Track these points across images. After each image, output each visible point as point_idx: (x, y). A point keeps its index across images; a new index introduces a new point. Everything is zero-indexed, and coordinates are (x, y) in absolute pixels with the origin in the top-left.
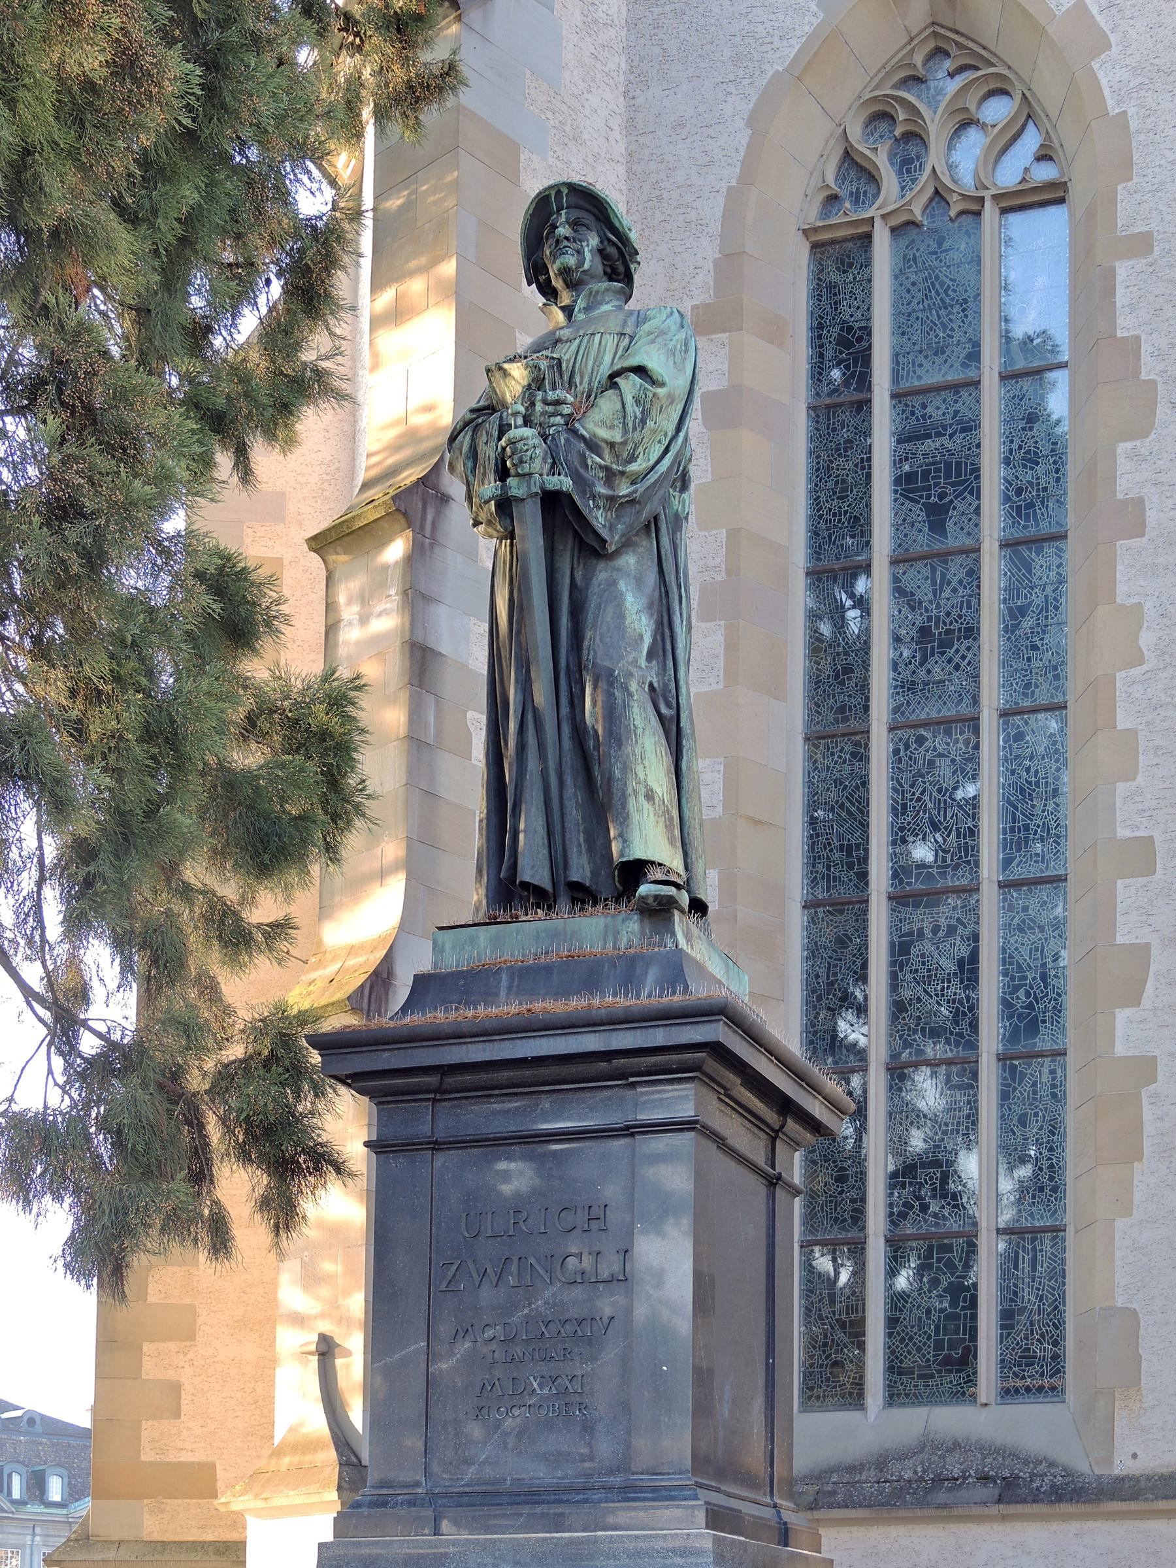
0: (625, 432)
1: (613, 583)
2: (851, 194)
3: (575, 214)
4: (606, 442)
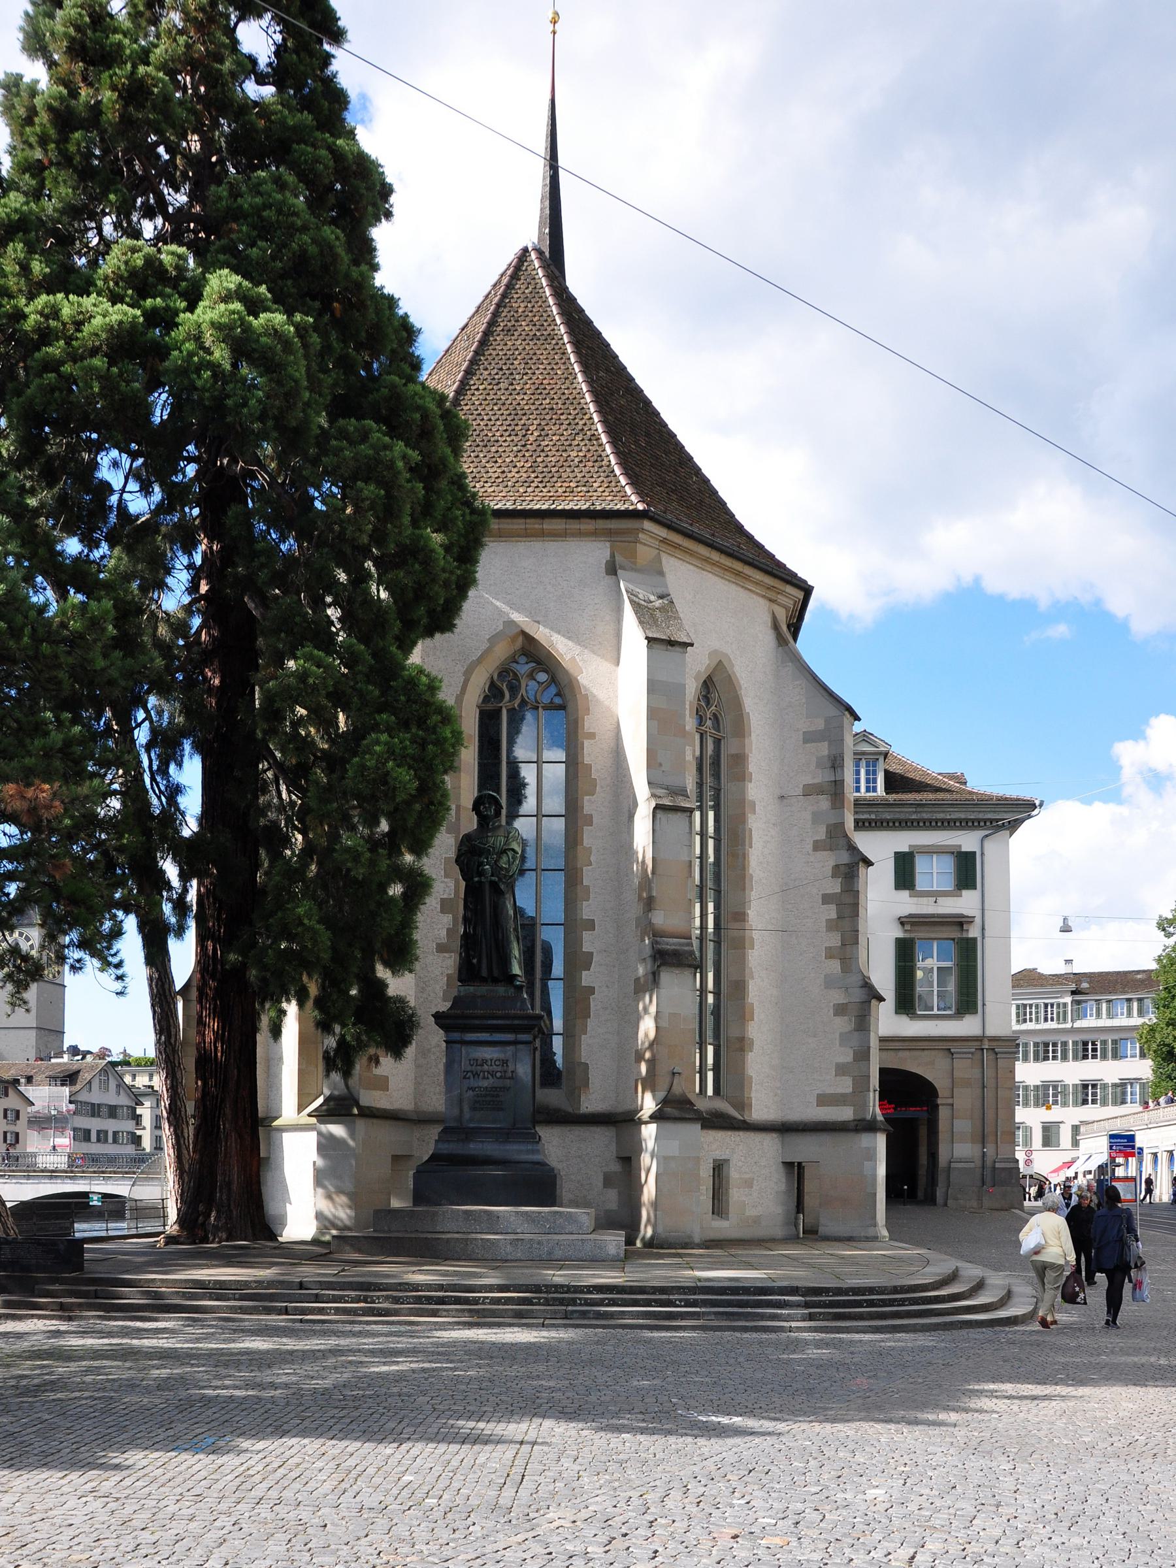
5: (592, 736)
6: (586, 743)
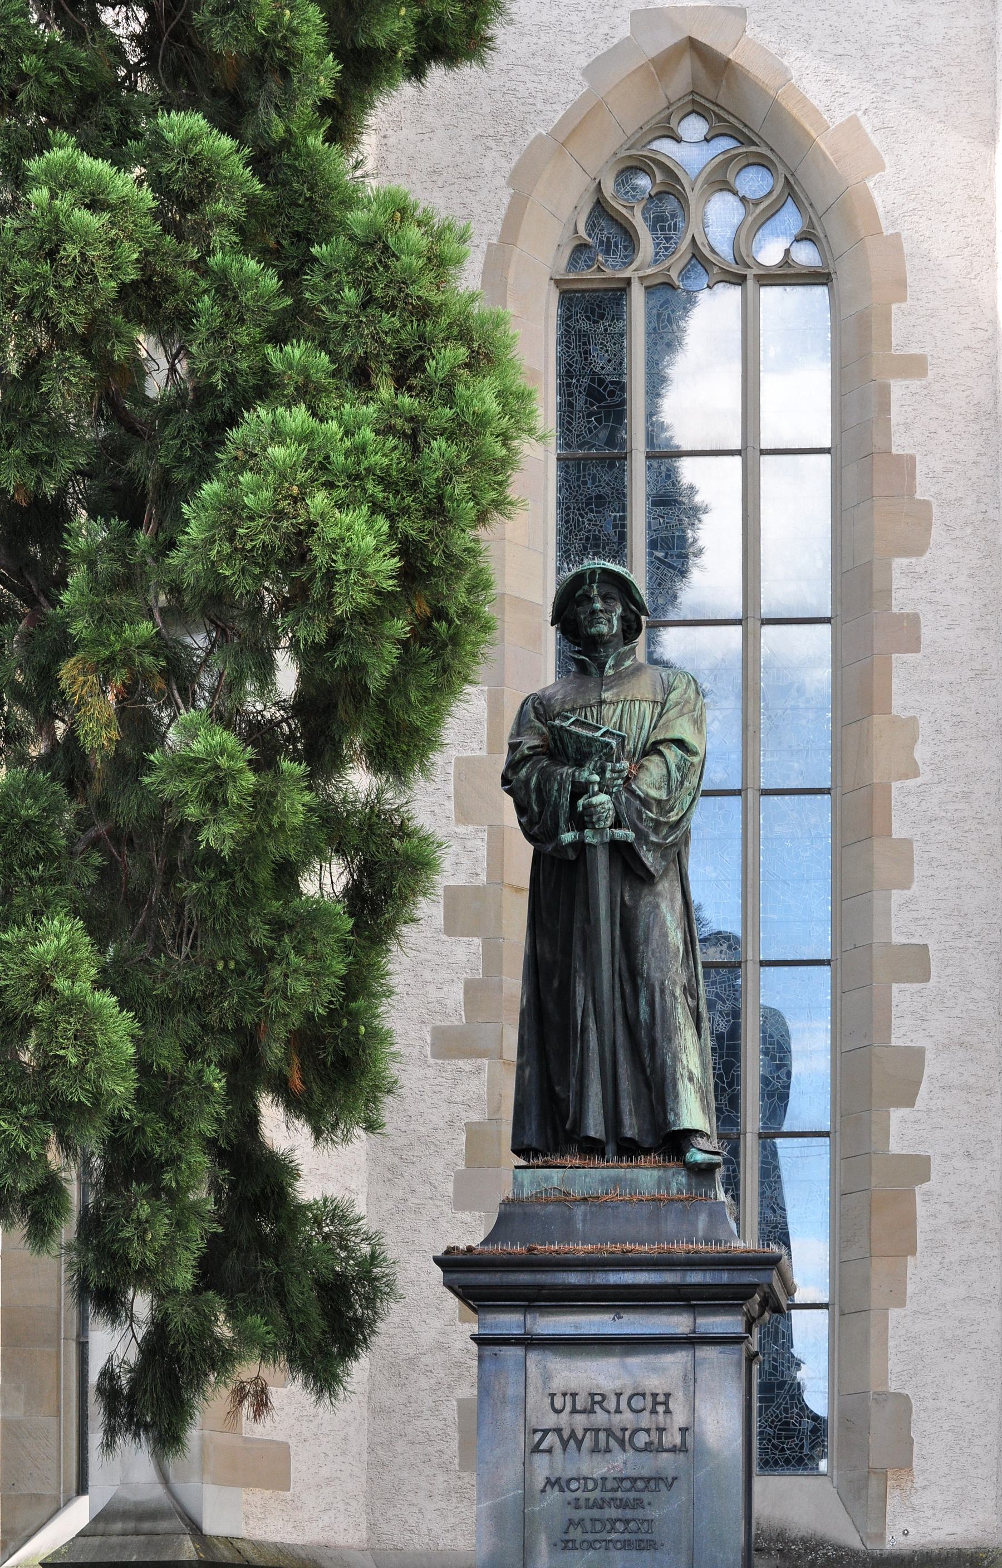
0: (669, 792)
1: (657, 906)
2: (601, 242)
3: (606, 589)
4: (655, 799)
5: (914, 366)
6: (898, 389)
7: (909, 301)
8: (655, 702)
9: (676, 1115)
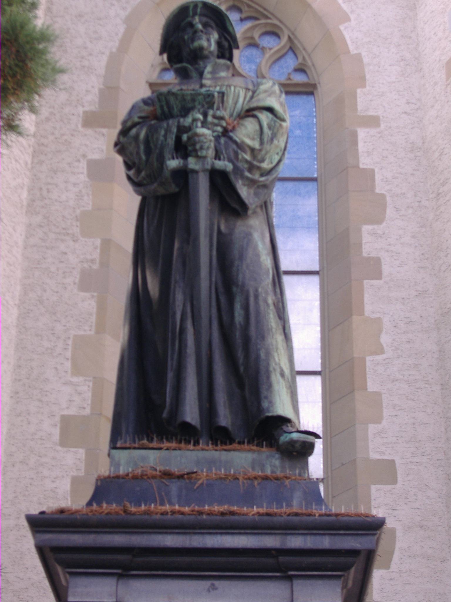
0: (262, 143)
5: (373, 121)
6: (362, 133)
7: (368, 88)
8: (247, 89)
9: (270, 402)
